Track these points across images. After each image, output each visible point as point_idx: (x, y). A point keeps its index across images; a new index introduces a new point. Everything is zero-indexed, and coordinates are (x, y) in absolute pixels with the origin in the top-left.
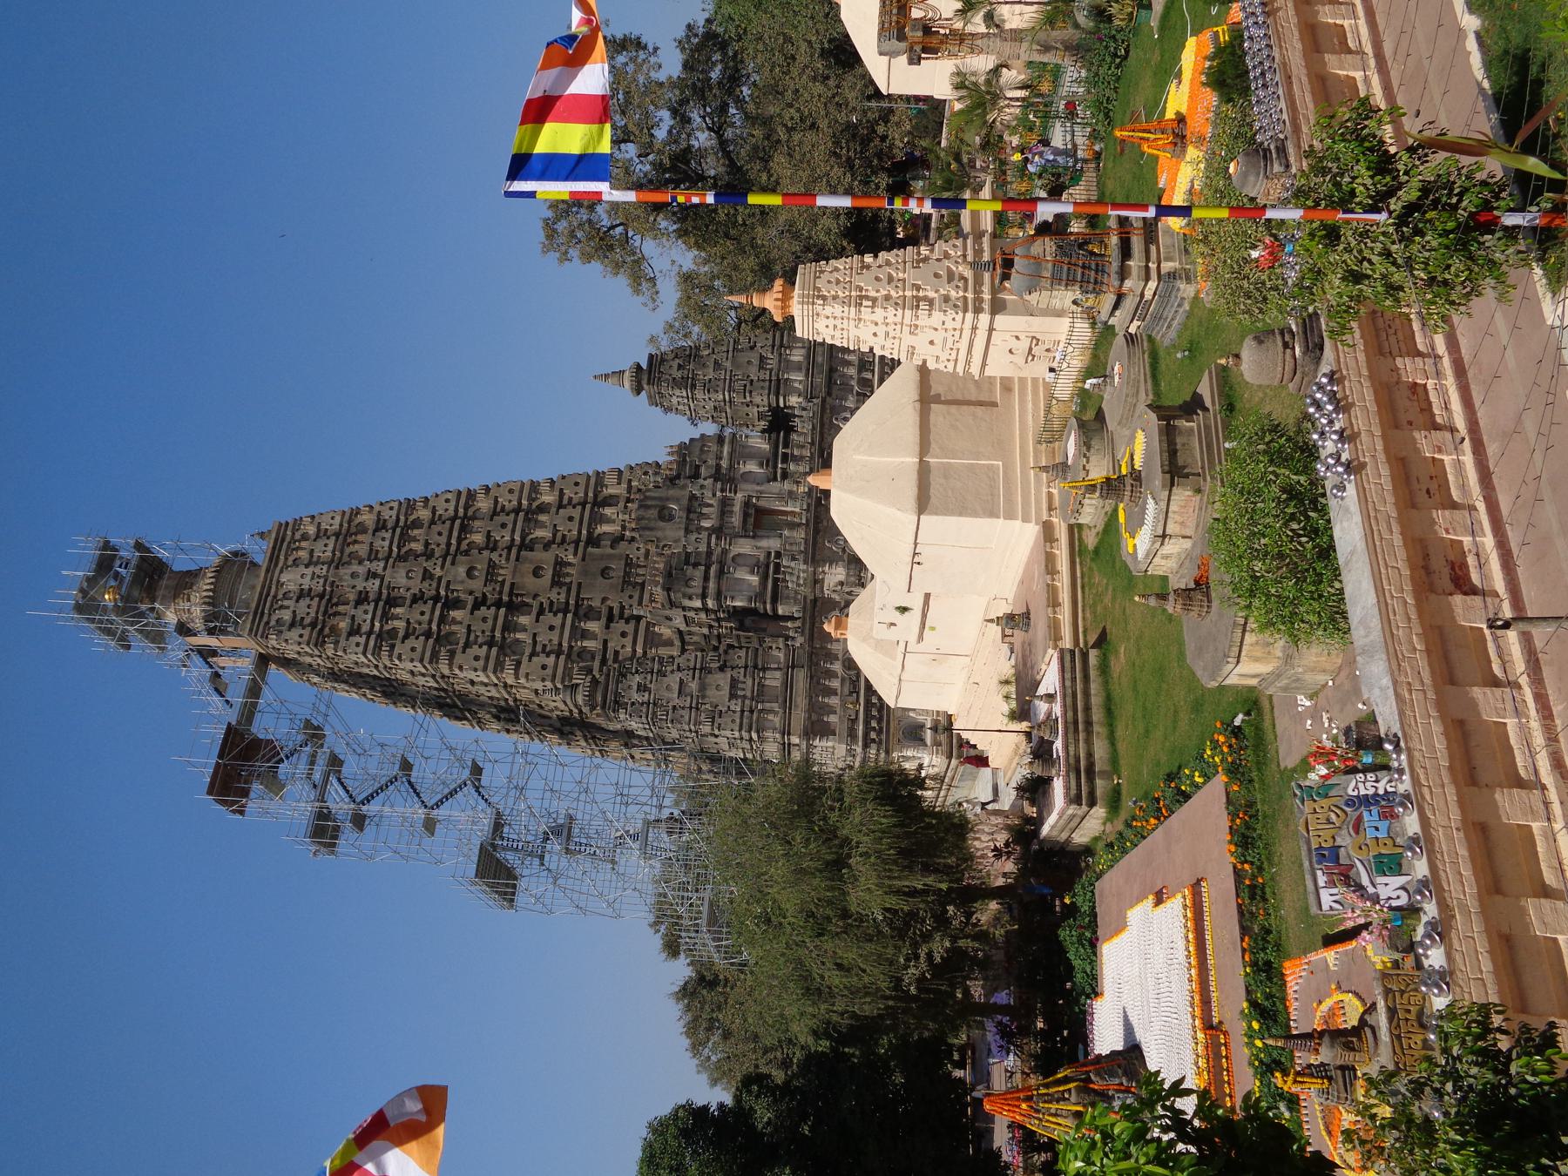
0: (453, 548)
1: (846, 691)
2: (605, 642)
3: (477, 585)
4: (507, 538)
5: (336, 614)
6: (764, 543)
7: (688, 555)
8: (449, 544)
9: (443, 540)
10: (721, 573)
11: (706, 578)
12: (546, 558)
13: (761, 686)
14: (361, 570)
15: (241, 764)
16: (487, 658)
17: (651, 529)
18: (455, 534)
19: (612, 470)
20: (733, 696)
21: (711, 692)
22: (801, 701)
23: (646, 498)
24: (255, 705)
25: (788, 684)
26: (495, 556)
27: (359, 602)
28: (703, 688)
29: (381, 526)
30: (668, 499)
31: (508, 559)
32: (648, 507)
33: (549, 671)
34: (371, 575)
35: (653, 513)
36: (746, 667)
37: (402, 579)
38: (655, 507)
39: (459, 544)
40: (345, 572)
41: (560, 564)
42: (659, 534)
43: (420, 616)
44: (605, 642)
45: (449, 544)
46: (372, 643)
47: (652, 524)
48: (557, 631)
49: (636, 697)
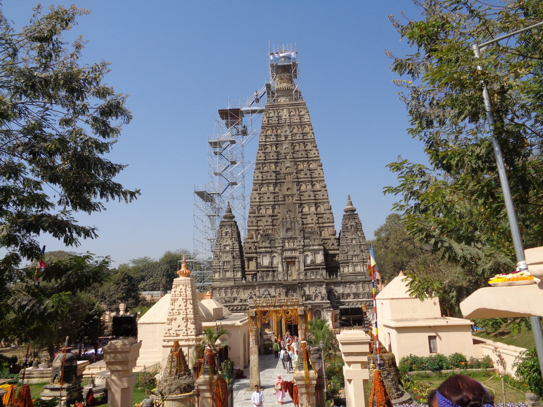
0: (297, 160)
1: (226, 299)
2: (264, 216)
3: (284, 171)
4: (302, 177)
5: (273, 130)
6: (280, 266)
7: (275, 240)
8: (298, 158)
9: (300, 156)
10: (268, 252)
11: (265, 248)
12: (295, 191)
13: (228, 271)
14: (288, 133)
15: (231, 116)
17: (283, 226)
18: (302, 159)
20: (224, 262)
21: (225, 255)
22: (223, 284)
23: (295, 223)
24: (249, 113)
25: (228, 279)
26: (294, 174)
27: (277, 135)
28: (227, 252)
29: (304, 134)
30: (295, 230)
31: (293, 179)
32: (291, 224)
33: (254, 200)
34: (286, 137)
35: (289, 226)
36: (234, 265)
37: (285, 147)
39: (299, 161)
40: (287, 128)
41: (292, 196)
42: (281, 230)
43: (273, 156)
44: (264, 216)
45: (298, 158)
46: (263, 143)
48: (268, 200)
49: (224, 232)
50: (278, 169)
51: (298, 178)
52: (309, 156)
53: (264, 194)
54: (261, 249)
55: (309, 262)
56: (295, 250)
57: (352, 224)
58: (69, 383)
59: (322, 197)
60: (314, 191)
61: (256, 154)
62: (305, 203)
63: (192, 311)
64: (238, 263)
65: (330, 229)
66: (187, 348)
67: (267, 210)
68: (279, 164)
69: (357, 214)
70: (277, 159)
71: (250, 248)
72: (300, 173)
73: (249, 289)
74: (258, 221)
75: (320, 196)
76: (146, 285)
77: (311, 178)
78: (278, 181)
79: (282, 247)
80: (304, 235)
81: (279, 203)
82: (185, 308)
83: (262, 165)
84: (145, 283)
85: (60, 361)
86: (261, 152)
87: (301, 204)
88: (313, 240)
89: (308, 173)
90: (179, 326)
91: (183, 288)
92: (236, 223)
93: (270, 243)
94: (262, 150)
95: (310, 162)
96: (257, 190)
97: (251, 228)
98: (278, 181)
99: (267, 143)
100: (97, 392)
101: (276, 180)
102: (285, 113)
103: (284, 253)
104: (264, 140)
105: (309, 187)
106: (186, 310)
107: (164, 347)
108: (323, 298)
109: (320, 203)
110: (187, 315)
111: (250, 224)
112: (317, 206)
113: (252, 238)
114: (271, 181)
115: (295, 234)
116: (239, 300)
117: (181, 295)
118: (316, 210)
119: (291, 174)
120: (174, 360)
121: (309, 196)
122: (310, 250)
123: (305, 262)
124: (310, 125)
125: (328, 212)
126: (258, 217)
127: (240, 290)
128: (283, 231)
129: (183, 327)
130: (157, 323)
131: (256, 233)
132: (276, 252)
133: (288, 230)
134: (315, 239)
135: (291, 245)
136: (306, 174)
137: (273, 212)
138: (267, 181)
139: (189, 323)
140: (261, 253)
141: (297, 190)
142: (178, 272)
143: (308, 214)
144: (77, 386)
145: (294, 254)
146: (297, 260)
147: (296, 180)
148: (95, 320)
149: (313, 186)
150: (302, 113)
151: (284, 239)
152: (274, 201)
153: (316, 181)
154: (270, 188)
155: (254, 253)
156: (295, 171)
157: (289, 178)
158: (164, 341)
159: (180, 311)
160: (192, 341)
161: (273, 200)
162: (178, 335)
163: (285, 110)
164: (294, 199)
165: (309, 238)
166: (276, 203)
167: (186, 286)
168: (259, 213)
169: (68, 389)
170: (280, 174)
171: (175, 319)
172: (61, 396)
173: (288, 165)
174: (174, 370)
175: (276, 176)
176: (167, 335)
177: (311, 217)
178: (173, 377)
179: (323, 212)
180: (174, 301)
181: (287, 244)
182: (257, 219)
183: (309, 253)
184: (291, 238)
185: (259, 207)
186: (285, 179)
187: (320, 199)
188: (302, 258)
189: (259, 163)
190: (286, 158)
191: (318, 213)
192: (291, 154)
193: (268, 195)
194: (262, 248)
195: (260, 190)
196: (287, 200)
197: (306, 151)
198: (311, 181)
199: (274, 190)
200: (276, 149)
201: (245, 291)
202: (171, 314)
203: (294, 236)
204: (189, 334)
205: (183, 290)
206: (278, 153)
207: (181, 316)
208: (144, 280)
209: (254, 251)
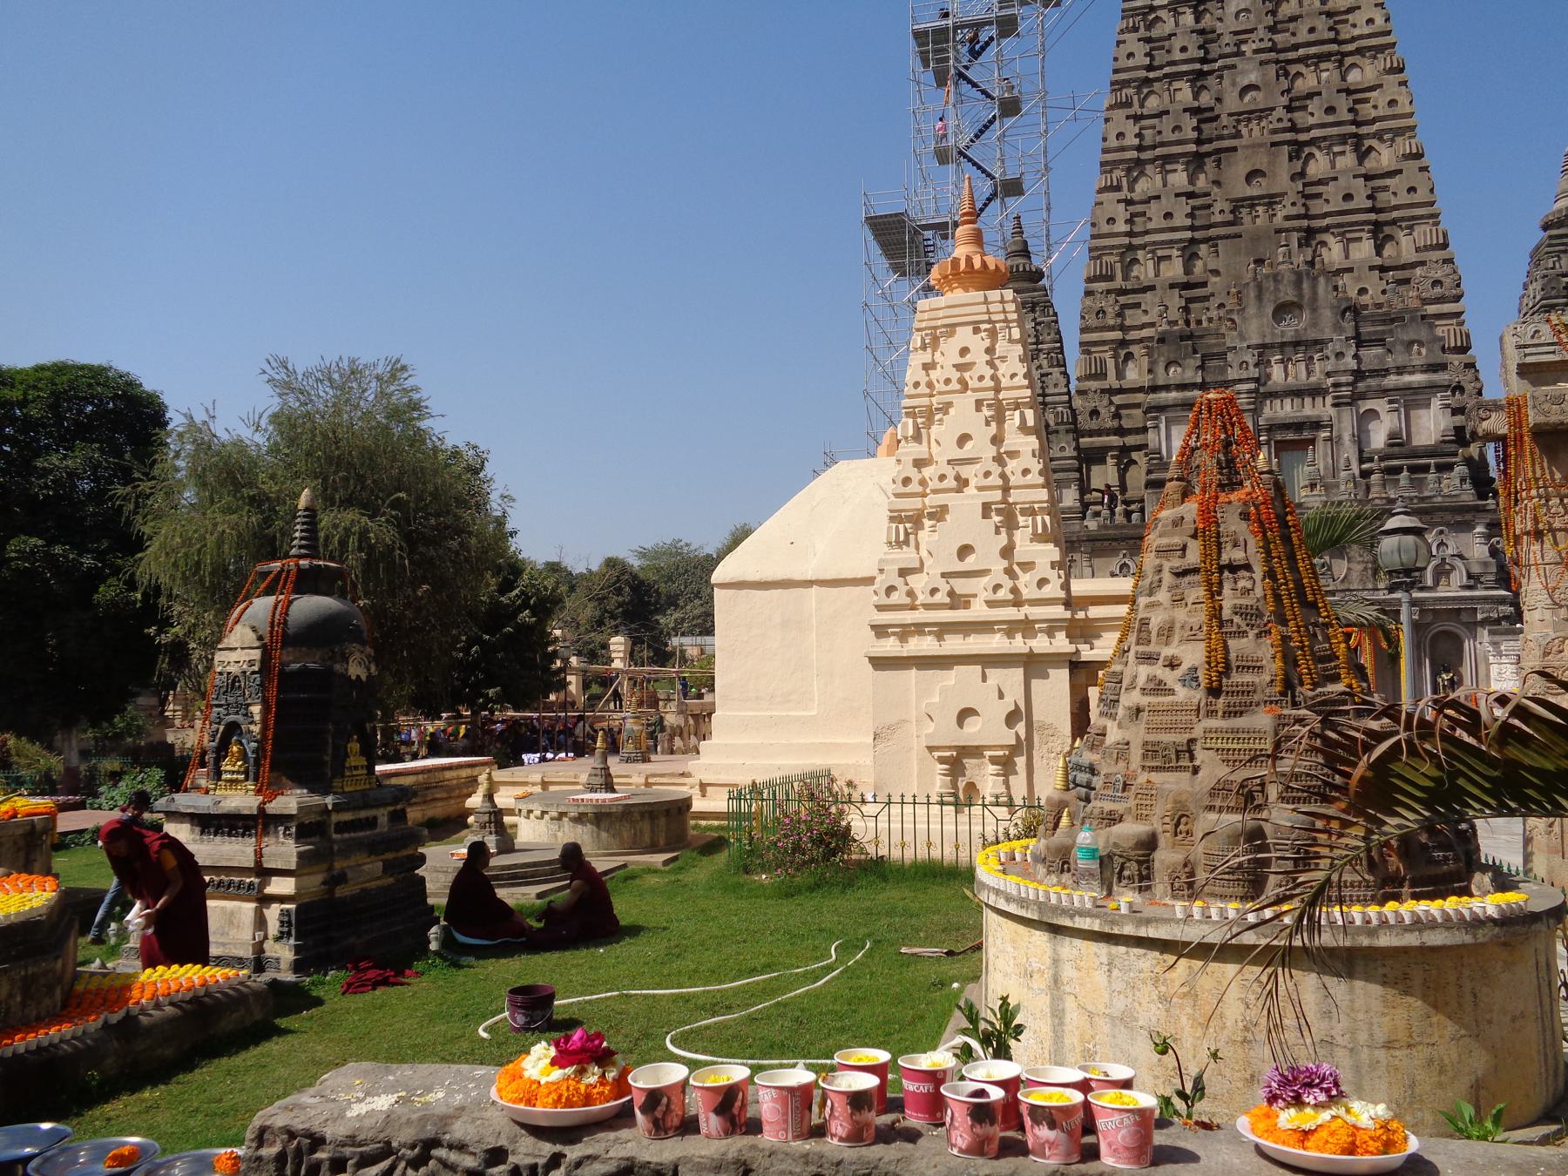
0: (1291, 55)
2: (1152, 288)
3: (1232, 103)
4: (1311, 121)
7: (1222, 356)
8: (1296, 47)
9: (1303, 36)
11: (1182, 387)
12: (1281, 178)
16: (1123, 149)
17: (1259, 298)
18: (1313, 50)
23: (1315, 279)
30: (1314, 310)
31: (1275, 132)
33: (1105, 229)
35: (1288, 294)
38: (1301, 296)
41: (1271, 200)
42: (1252, 310)
44: (1152, 288)
45: (1296, 47)
47: (1267, 296)
50: (1206, 99)
51: (1293, 128)
52: (1343, 36)
53: (1147, 201)
56: (1316, 392)
58: (314, 780)
59: (1403, 198)
60: (1368, 177)
61: (1113, 50)
62: (1326, 229)
63: (1036, 466)
66: (1018, 674)
67: (1163, 265)
68: (1211, 81)
71: (1095, 413)
72: (1305, 108)
73: (1112, 552)
74: (1124, 307)
76: (683, 620)
77: (1354, 123)
78: (1206, 148)
79: (1257, 380)
80: (1357, 328)
81: (1212, 232)
82: (992, 451)
83: (1139, 89)
84: (677, 615)
85: (250, 637)
87: (1310, 233)
88: (1399, 348)
89: (1343, 103)
90: (965, 551)
91: (978, 344)
93: (1202, 367)
94: (1135, 29)
95: (1348, 61)
96: (1118, 188)
97: (1095, 336)
98: (1206, 148)
100: (518, 877)
101: (1199, 142)
103: (1267, 410)
105: (1347, 161)
106: (999, 459)
107: (879, 663)
108: (1474, 580)
109: (1394, 222)
110: (1006, 489)
111: (1092, 321)
112: (1381, 235)
113: (1103, 376)
115: (1314, 324)
117: (962, 382)
118: (1379, 254)
119: (1262, 113)
120: (1231, 554)
122: (1384, 392)
123: (1360, 439)
126: (1122, 292)
127: (1077, 556)
128: (1260, 315)
130: (809, 583)
131: (1115, 357)
133: (1282, 310)
134: (1411, 343)
135: (1299, 374)
136: (1330, 110)
137: (1188, 272)
138: (1159, 151)
139: (1022, 537)
140: (1161, 408)
141: (1293, 178)
144: (382, 815)
145: (1310, 409)
146: (1324, 434)
147: (1288, 136)
148: (523, 628)
149: (1363, 155)
151: (1264, 346)
152: (1192, 228)
153: (1378, 135)
154: (1170, 177)
155: (1108, 432)
156: (1284, 100)
157: (1256, 132)
158: (880, 631)
159: (967, 471)
160: (1050, 633)
161: (1188, 222)
162: (958, 601)
164: (1280, 215)
165: (1380, 342)
166: (1198, 235)
167: (993, 334)
168: (1126, 278)
169: (306, 828)
170: (1218, 116)
171: (939, 514)
172: (265, 873)
173: (1253, 77)
174: (1259, 652)
175: (1197, 129)
176: (896, 598)
177: (1358, 279)
178: (1262, 720)
181: (1277, 373)
182: (1122, 300)
183: (1380, 405)
184: (1296, 344)
185: (1128, 257)
186: (1238, 135)
187: (1397, 208)
188: (1346, 423)
189: (1125, 84)
190: (1239, 54)
191: (1387, 263)
192: (1261, 33)
193: (1167, 203)
194: (1167, 388)
195: (1131, 190)
196: (1247, 219)
197: (1329, 14)
198: (1356, 135)
199: (1192, 181)
200: (1197, 20)
201: (1096, 562)
202: (914, 487)
203: (1312, 335)
204: (1027, 593)
205: (978, 356)
206: (1207, 36)
207: (972, 499)
208: (677, 606)
209: (1110, 424)
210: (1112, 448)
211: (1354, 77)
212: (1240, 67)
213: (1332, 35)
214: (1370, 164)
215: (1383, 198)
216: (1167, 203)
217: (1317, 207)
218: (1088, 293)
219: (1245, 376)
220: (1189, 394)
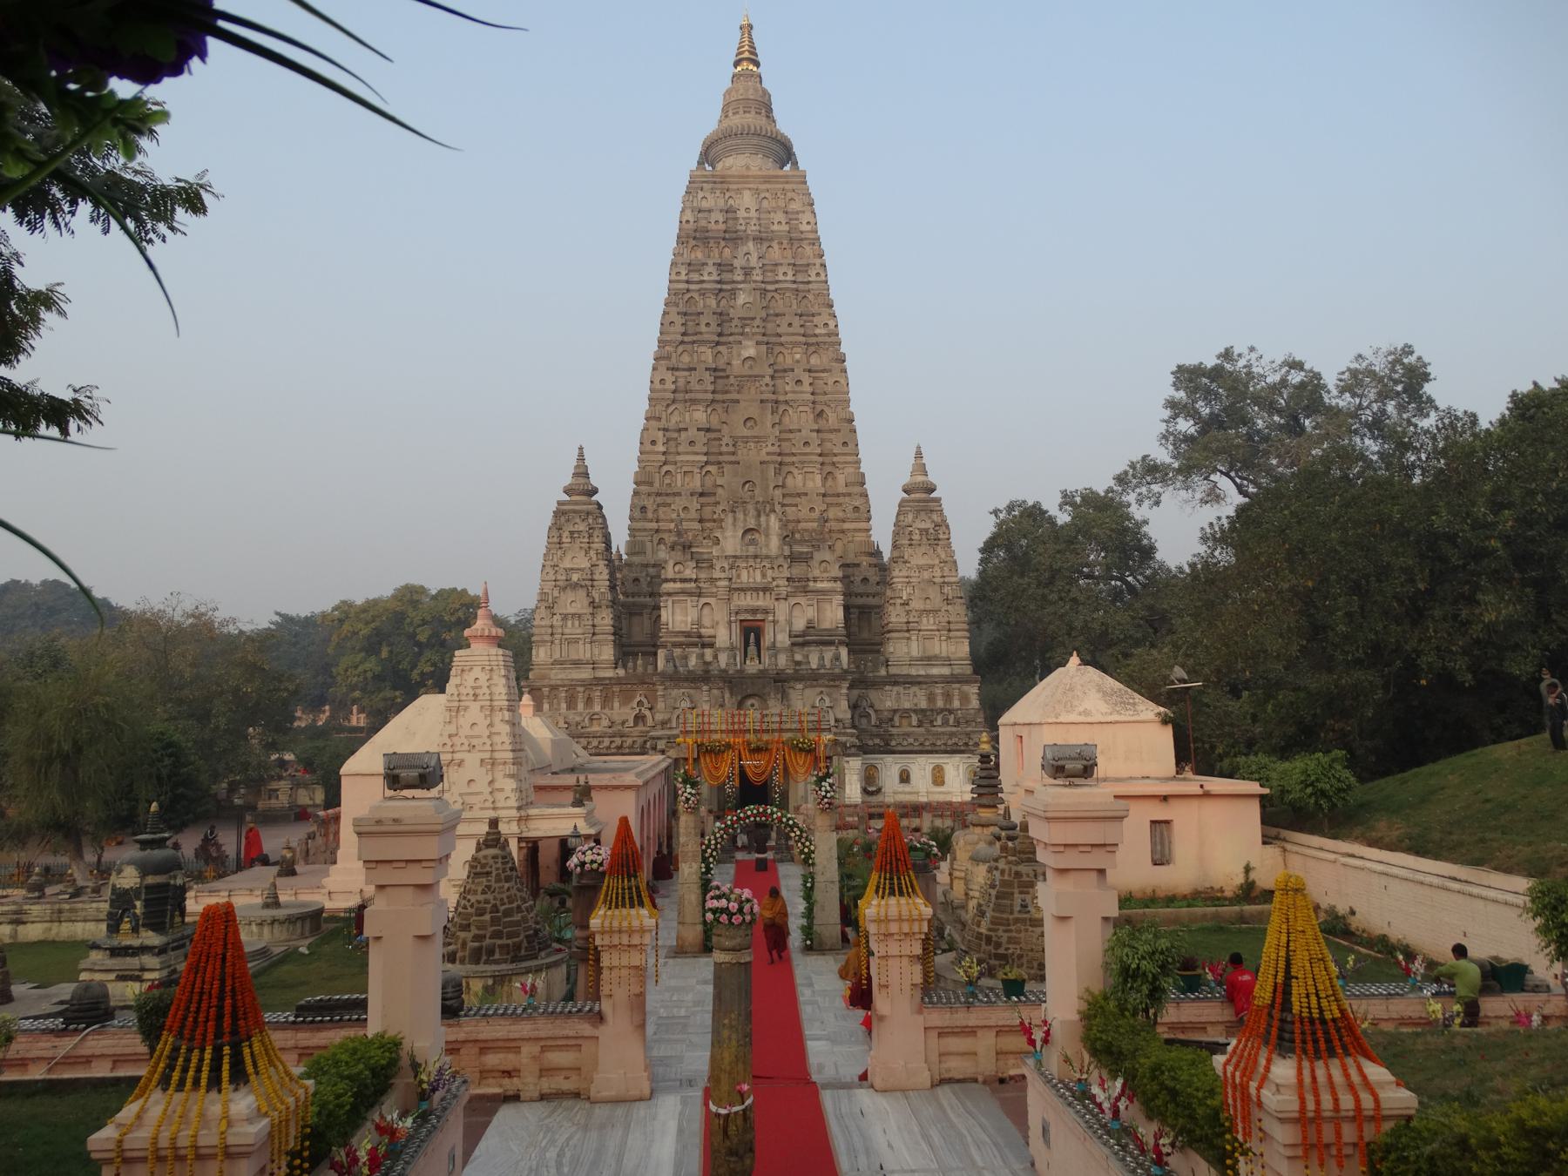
2: (679, 494)
14: (754, 261)
17: (734, 525)
19: (863, 475)
20: (565, 617)
25: (577, 663)
26: (767, 379)
34: (747, 271)
42: (729, 533)
44: (679, 494)
48: (690, 449)
54: (671, 585)
55: (800, 625)
57: (923, 526)
64: (605, 619)
65: (860, 537)
69: (938, 500)
70: (720, 335)
75: (834, 443)
81: (721, 458)
86: (674, 310)
92: (600, 507)
95: (812, 349)
99: (692, 287)
102: (746, 202)
104: (683, 277)
114: (700, 396)
116: (605, 723)
121: (806, 443)
124: (816, 241)
125: (856, 489)
126: (659, 494)
129: (482, 786)
132: (713, 595)
142: (467, 632)
143: (799, 495)
150: (794, 206)
151: (735, 557)
156: (770, 371)
161: (705, 449)
163: (747, 195)
168: (661, 484)
179: (842, 490)
180: (456, 710)
182: (659, 500)
194: (674, 580)
205: (483, 681)
210: (644, 606)
211: (814, 360)
212: (745, 343)
213: (802, 331)
214: (822, 424)
215: (828, 445)
216: (692, 432)
217: (786, 447)
218: (636, 493)
219: (723, 575)
220: (687, 585)
